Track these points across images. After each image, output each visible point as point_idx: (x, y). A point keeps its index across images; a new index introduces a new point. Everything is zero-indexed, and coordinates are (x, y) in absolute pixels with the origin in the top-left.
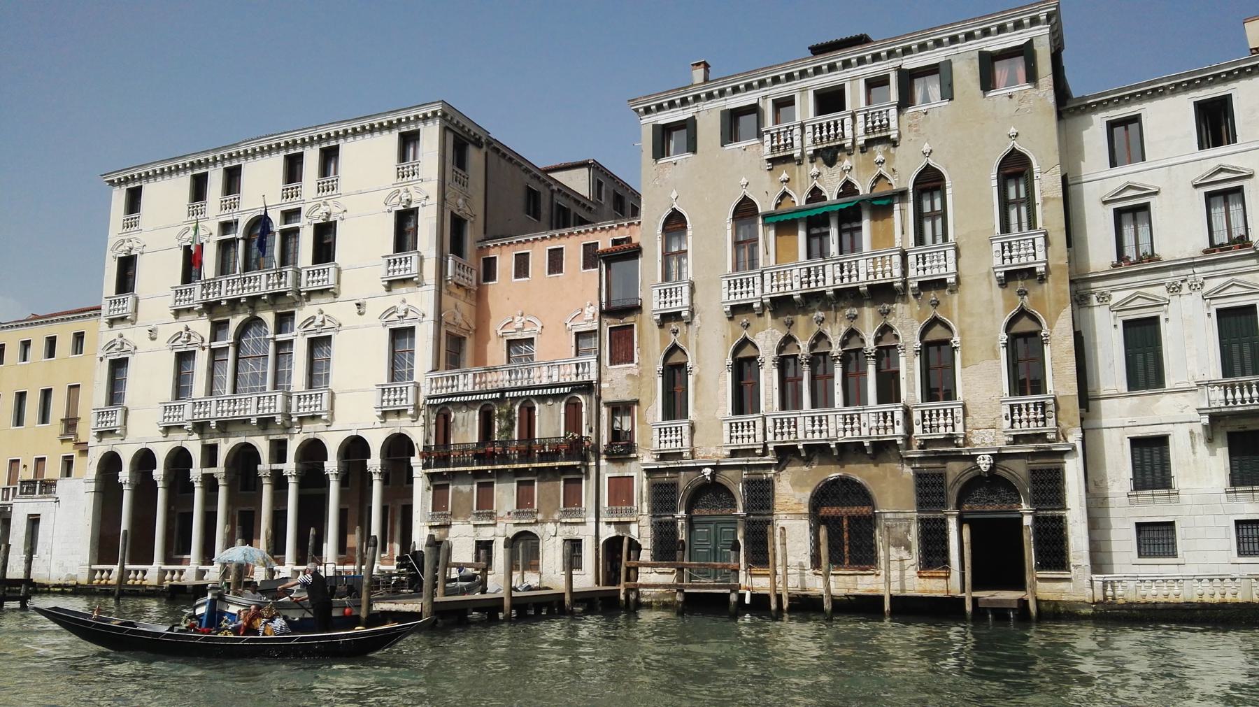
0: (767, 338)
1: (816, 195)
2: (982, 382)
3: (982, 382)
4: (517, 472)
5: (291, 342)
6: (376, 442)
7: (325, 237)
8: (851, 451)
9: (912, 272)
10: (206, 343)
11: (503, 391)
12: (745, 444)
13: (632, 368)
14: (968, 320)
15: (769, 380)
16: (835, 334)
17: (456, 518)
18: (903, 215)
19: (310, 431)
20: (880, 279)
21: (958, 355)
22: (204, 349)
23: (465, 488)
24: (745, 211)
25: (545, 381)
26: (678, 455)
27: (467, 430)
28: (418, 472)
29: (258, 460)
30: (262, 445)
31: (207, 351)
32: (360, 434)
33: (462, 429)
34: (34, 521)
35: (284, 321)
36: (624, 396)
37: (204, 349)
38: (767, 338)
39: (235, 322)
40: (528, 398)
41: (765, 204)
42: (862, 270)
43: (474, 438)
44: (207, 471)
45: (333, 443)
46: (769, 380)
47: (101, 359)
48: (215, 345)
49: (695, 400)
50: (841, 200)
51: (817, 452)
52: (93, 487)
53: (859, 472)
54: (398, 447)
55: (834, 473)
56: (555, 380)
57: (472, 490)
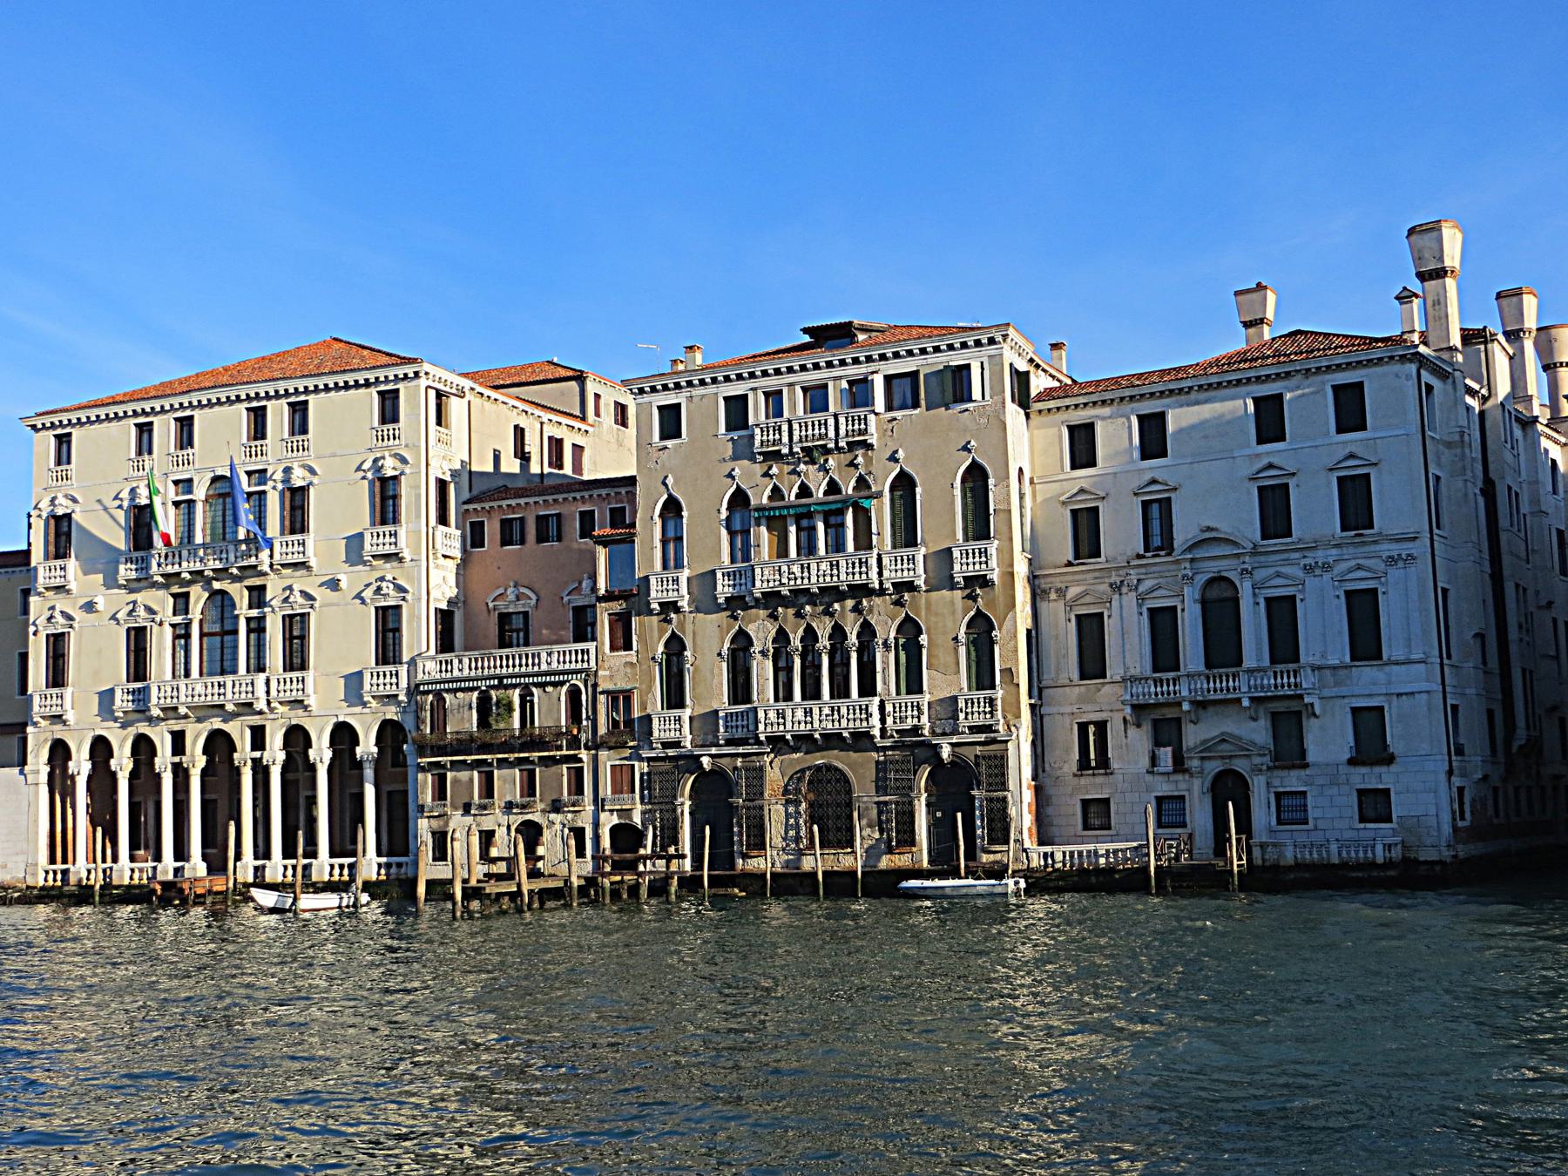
0: (761, 630)
1: (805, 491)
2: (946, 677)
3: (946, 677)
7: (296, 500)
8: (832, 740)
9: (886, 574)
11: (501, 678)
12: (739, 734)
13: (631, 656)
14: (933, 619)
15: (763, 672)
16: (823, 629)
18: (882, 514)
20: (858, 580)
21: (924, 652)
23: (463, 775)
24: (739, 499)
25: (544, 667)
26: (676, 744)
29: (232, 748)
36: (622, 685)
38: (761, 630)
40: (526, 686)
41: (761, 497)
42: (843, 570)
44: (177, 759)
46: (763, 672)
49: (693, 689)
50: (831, 498)
51: (805, 742)
53: (836, 759)
55: (819, 760)
56: (554, 665)
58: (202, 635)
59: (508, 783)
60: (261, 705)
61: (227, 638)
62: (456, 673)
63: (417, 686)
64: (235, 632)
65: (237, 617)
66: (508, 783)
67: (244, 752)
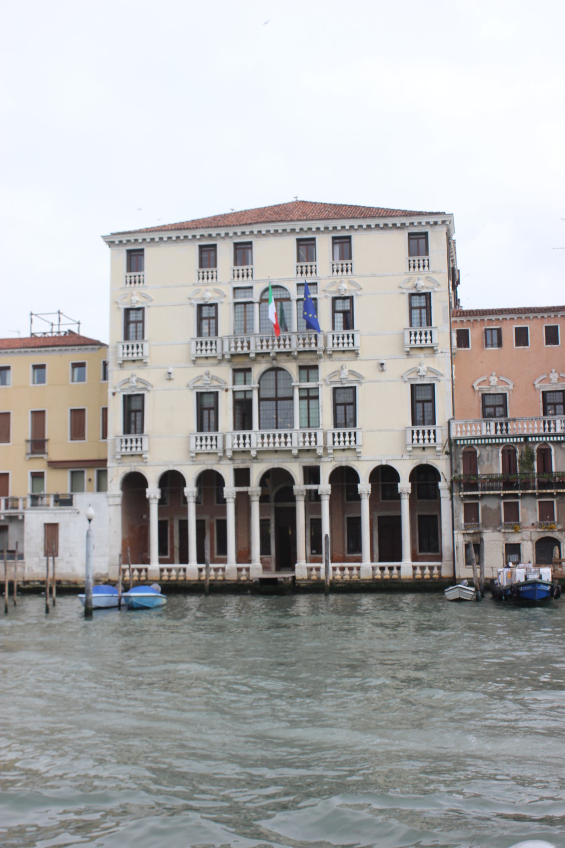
4: (541, 495)
5: (317, 388)
6: (404, 470)
10: (230, 386)
11: (526, 437)
17: (486, 527)
19: (343, 460)
22: (227, 390)
27: (492, 465)
28: (444, 494)
30: (296, 471)
31: (230, 393)
32: (391, 464)
33: (486, 463)
34: (52, 530)
35: (309, 370)
37: (227, 390)
39: (258, 370)
43: (498, 470)
45: (364, 472)
47: (114, 394)
48: (238, 388)
52: (119, 501)
54: (424, 476)
57: (499, 508)
58: (260, 400)
59: (529, 512)
60: (320, 451)
61: (312, 402)
62: (484, 433)
63: (456, 441)
64: (291, 398)
65: (293, 387)
66: (529, 512)
67: (300, 486)
